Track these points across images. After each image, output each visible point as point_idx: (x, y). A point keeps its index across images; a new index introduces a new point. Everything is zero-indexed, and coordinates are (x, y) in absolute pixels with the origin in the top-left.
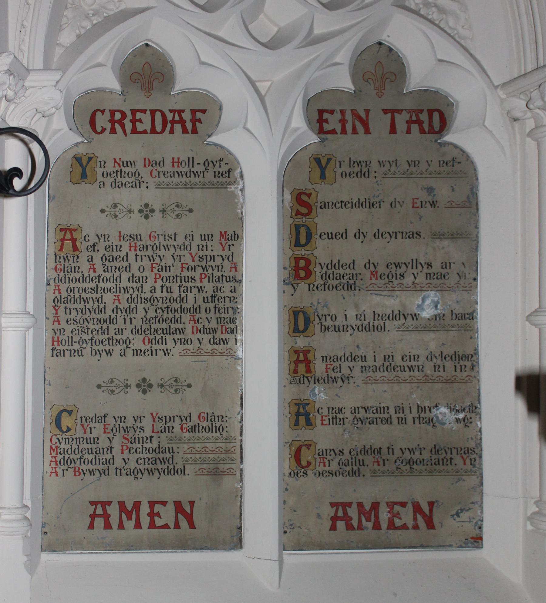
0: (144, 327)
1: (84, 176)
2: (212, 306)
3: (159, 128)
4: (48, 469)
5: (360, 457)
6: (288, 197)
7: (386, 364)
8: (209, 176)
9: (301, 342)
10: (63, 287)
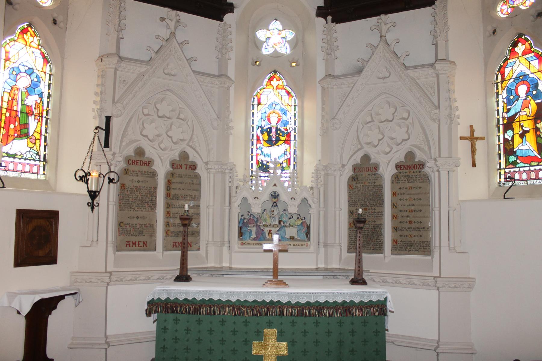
1: (126, 173)
3: (142, 164)
4: (118, 234)
6: (166, 181)
8: (151, 175)
9: (168, 210)
10: (122, 196)
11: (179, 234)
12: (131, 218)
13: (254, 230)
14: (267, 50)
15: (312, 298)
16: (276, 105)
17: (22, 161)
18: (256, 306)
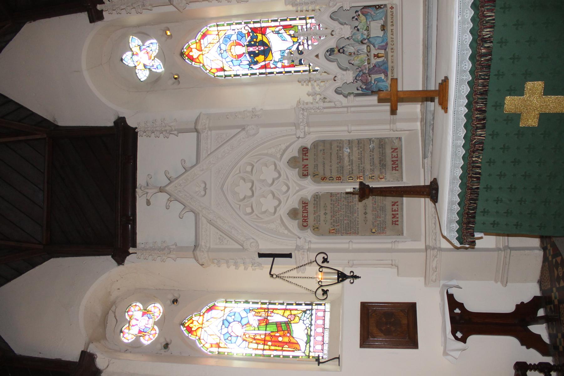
0: (352, 214)
2: (347, 199)
3: (307, 211)
5: (381, 164)
6: (322, 182)
7: (360, 159)
8: (317, 200)
11: (383, 164)
12: (366, 220)
13: (374, 77)
14: (159, 67)
15: (465, 52)
16: (221, 50)
17: (313, 328)
18: (473, 124)
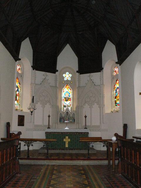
14: (65, 79)
